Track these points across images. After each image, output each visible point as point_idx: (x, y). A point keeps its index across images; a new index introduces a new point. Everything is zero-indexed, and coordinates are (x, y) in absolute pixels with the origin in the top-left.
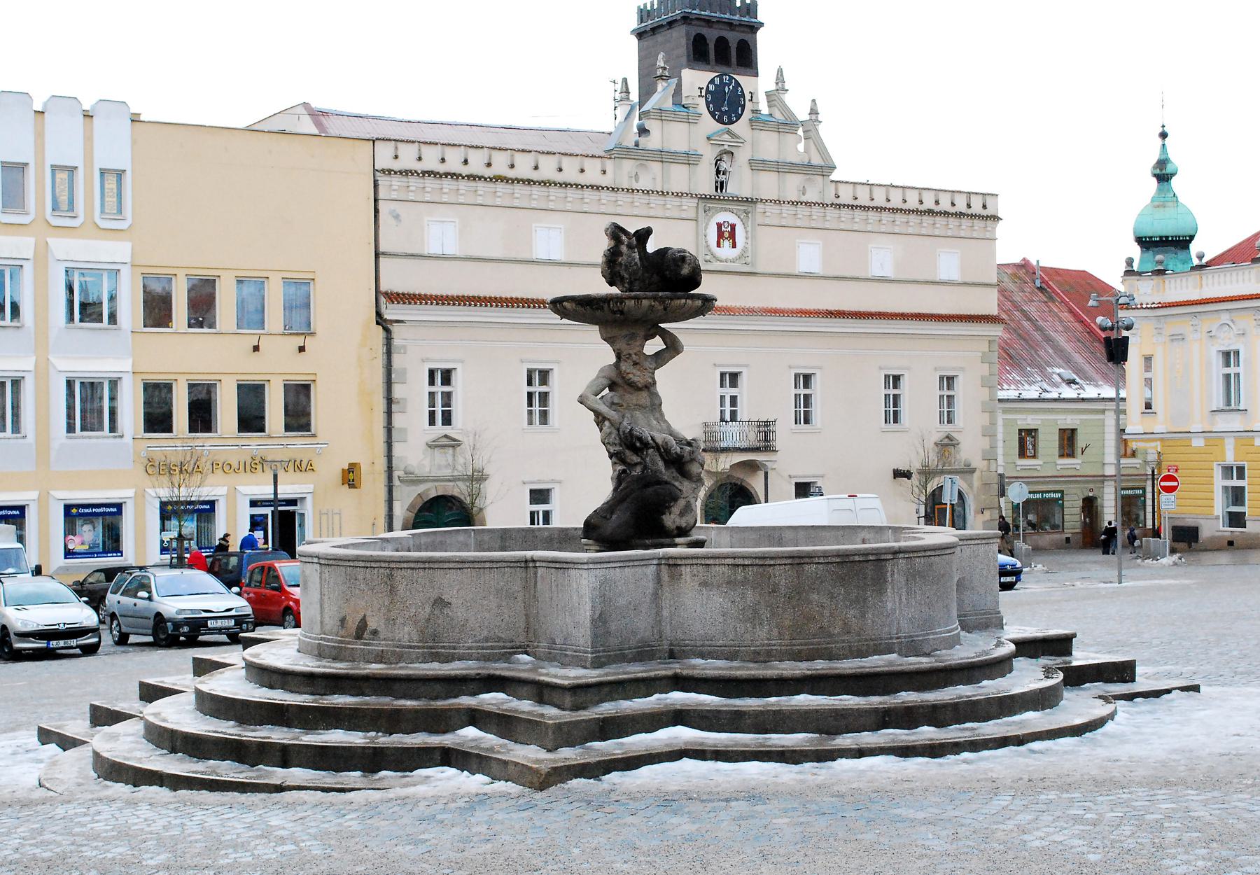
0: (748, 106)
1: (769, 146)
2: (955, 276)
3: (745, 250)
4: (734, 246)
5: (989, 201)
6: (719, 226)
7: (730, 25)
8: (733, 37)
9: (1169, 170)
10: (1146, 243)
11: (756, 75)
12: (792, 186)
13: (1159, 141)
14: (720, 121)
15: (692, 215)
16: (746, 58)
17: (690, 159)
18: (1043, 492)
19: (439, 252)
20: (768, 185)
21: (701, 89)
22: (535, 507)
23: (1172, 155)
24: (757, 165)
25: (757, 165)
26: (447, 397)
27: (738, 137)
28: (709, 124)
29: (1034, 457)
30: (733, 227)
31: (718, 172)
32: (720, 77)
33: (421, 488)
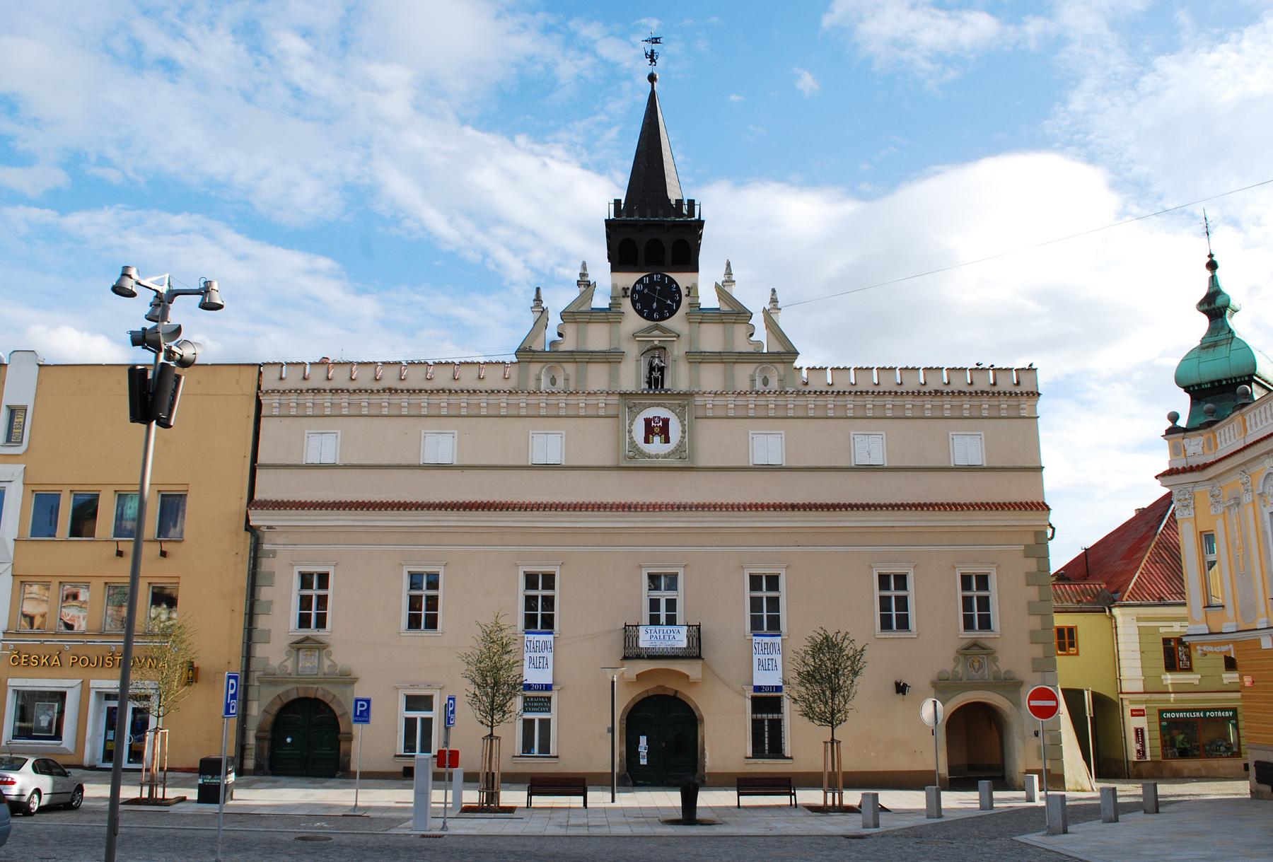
0: (685, 301)
1: (711, 338)
2: (977, 459)
3: (681, 443)
4: (667, 440)
5: (1025, 378)
6: (648, 421)
7: (660, 225)
8: (668, 240)
9: (1219, 302)
10: (1199, 392)
11: (696, 270)
12: (744, 375)
13: (1209, 274)
14: (649, 317)
15: (611, 412)
16: (688, 259)
17: (611, 357)
18: (1205, 710)
19: (316, 461)
20: (711, 378)
21: (625, 290)
22: (412, 714)
23: (1225, 285)
24: (697, 358)
25: (697, 358)
26: (323, 601)
27: (670, 331)
28: (633, 321)
29: (1190, 669)
30: (666, 421)
31: (652, 369)
32: (651, 277)
33: (280, 690)
